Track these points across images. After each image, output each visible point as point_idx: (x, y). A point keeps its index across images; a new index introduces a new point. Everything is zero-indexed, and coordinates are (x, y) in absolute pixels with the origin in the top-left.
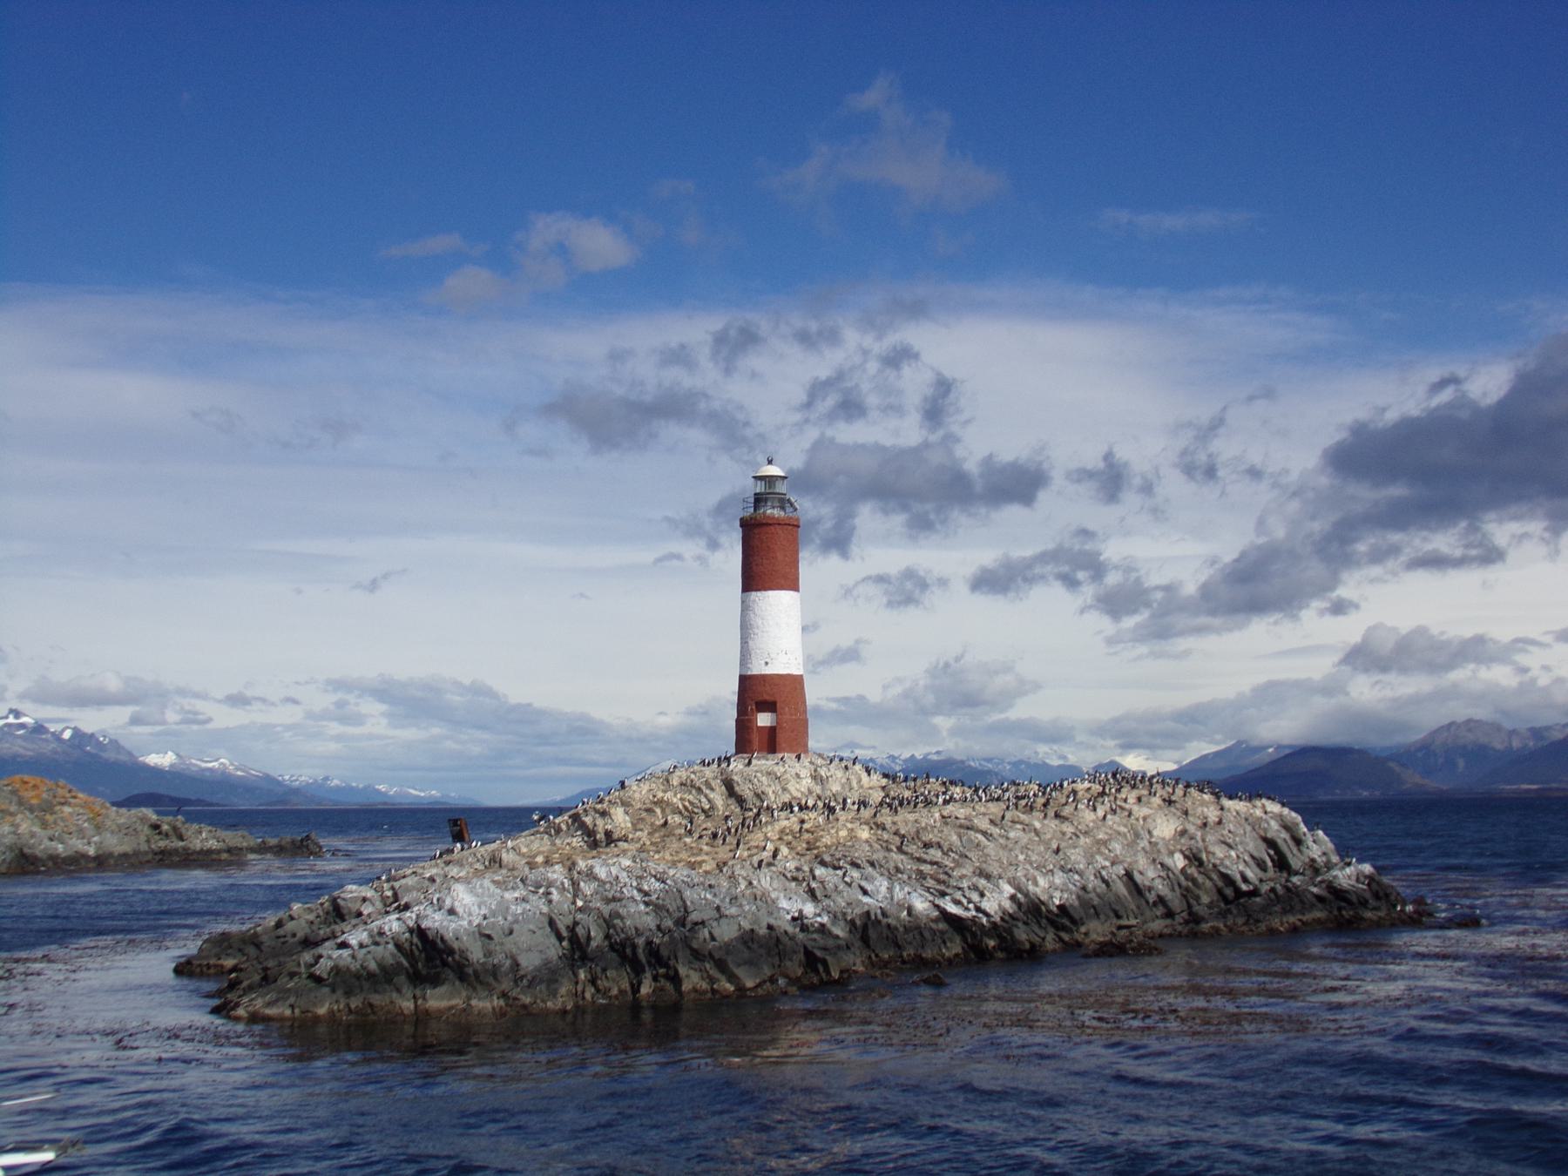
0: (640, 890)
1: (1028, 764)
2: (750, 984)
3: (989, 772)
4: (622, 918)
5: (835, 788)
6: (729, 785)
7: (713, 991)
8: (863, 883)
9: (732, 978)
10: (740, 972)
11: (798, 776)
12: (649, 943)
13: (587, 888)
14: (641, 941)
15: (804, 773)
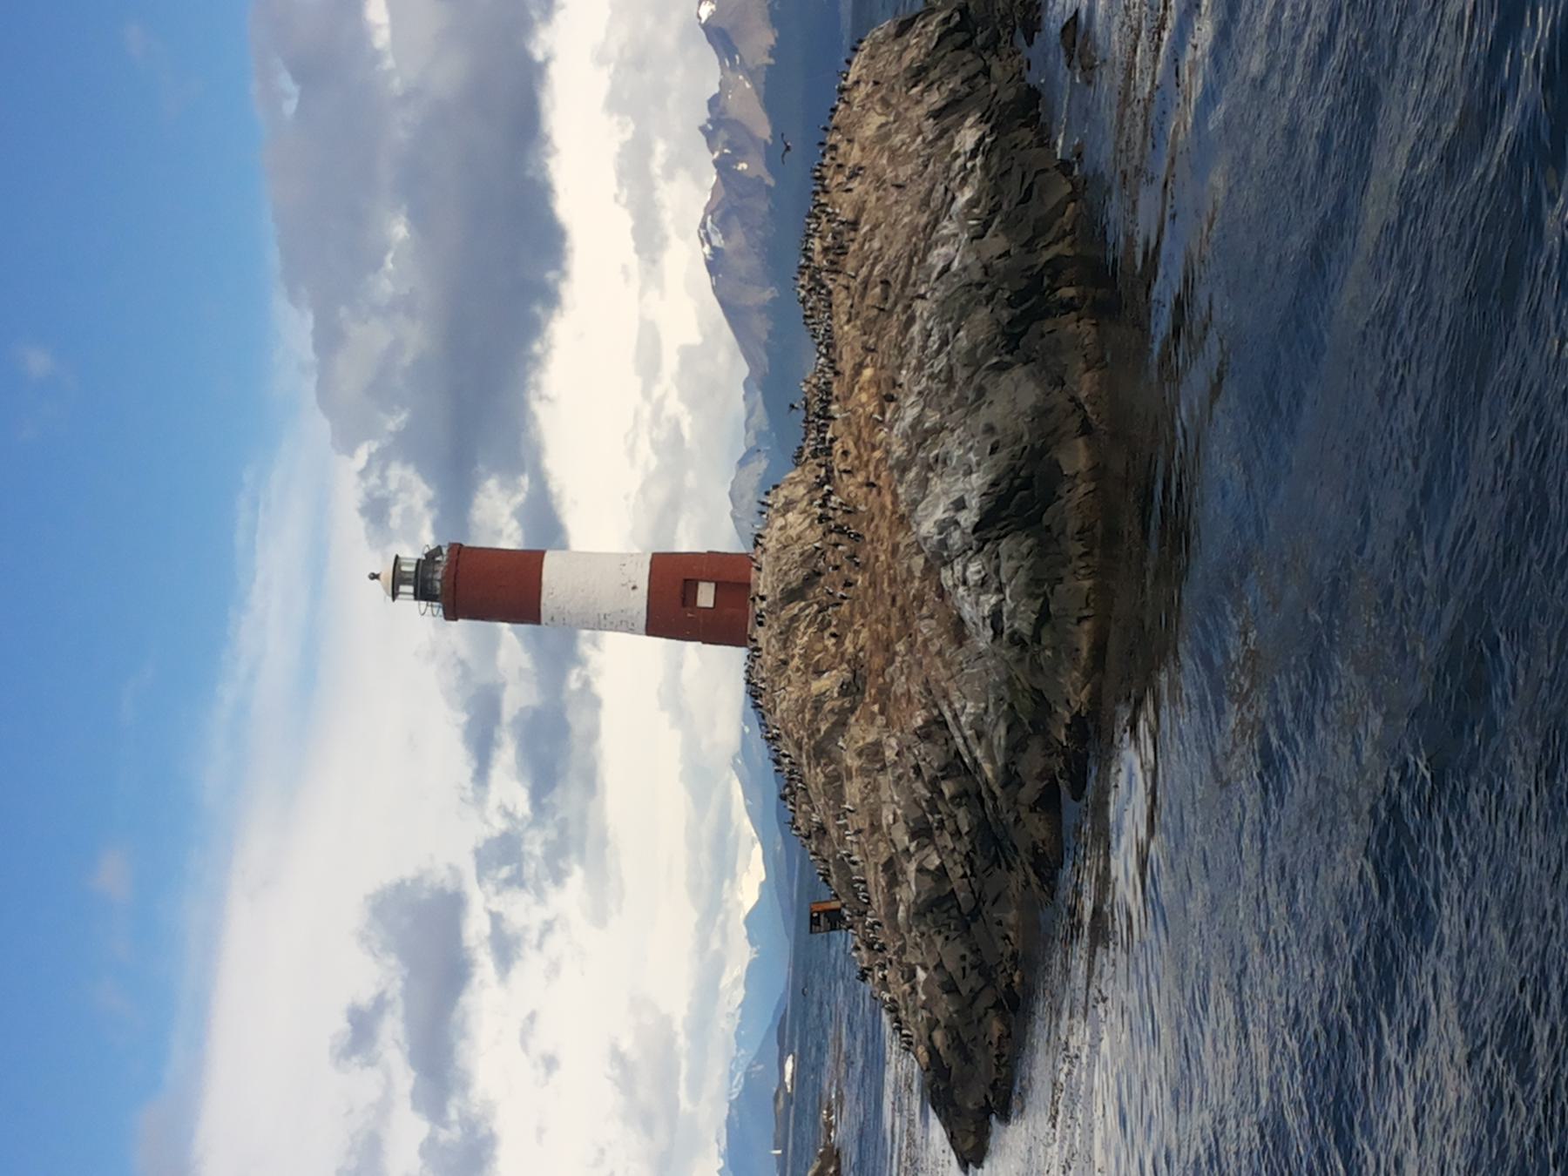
0: (939, 351)
1: (740, 1027)
2: (1069, 188)
3: (747, 1075)
4: (975, 347)
5: (801, 490)
6: (791, 595)
7: (1073, 231)
8: (935, 275)
9: (1059, 210)
10: (1052, 201)
11: (782, 528)
12: (1010, 303)
13: (933, 418)
14: (1005, 315)
15: (780, 522)
